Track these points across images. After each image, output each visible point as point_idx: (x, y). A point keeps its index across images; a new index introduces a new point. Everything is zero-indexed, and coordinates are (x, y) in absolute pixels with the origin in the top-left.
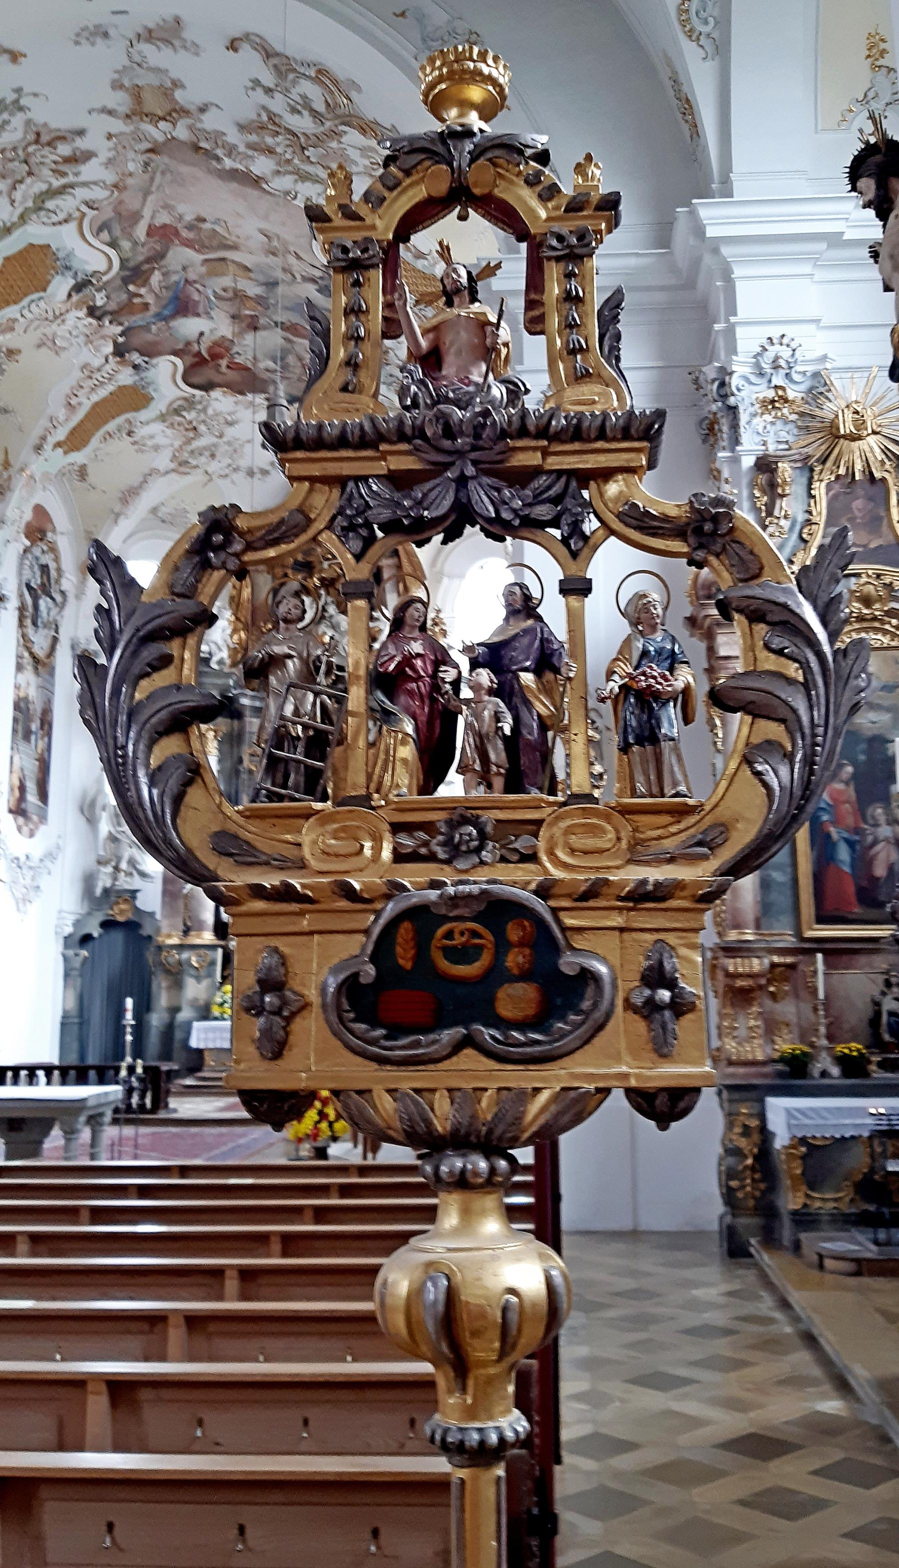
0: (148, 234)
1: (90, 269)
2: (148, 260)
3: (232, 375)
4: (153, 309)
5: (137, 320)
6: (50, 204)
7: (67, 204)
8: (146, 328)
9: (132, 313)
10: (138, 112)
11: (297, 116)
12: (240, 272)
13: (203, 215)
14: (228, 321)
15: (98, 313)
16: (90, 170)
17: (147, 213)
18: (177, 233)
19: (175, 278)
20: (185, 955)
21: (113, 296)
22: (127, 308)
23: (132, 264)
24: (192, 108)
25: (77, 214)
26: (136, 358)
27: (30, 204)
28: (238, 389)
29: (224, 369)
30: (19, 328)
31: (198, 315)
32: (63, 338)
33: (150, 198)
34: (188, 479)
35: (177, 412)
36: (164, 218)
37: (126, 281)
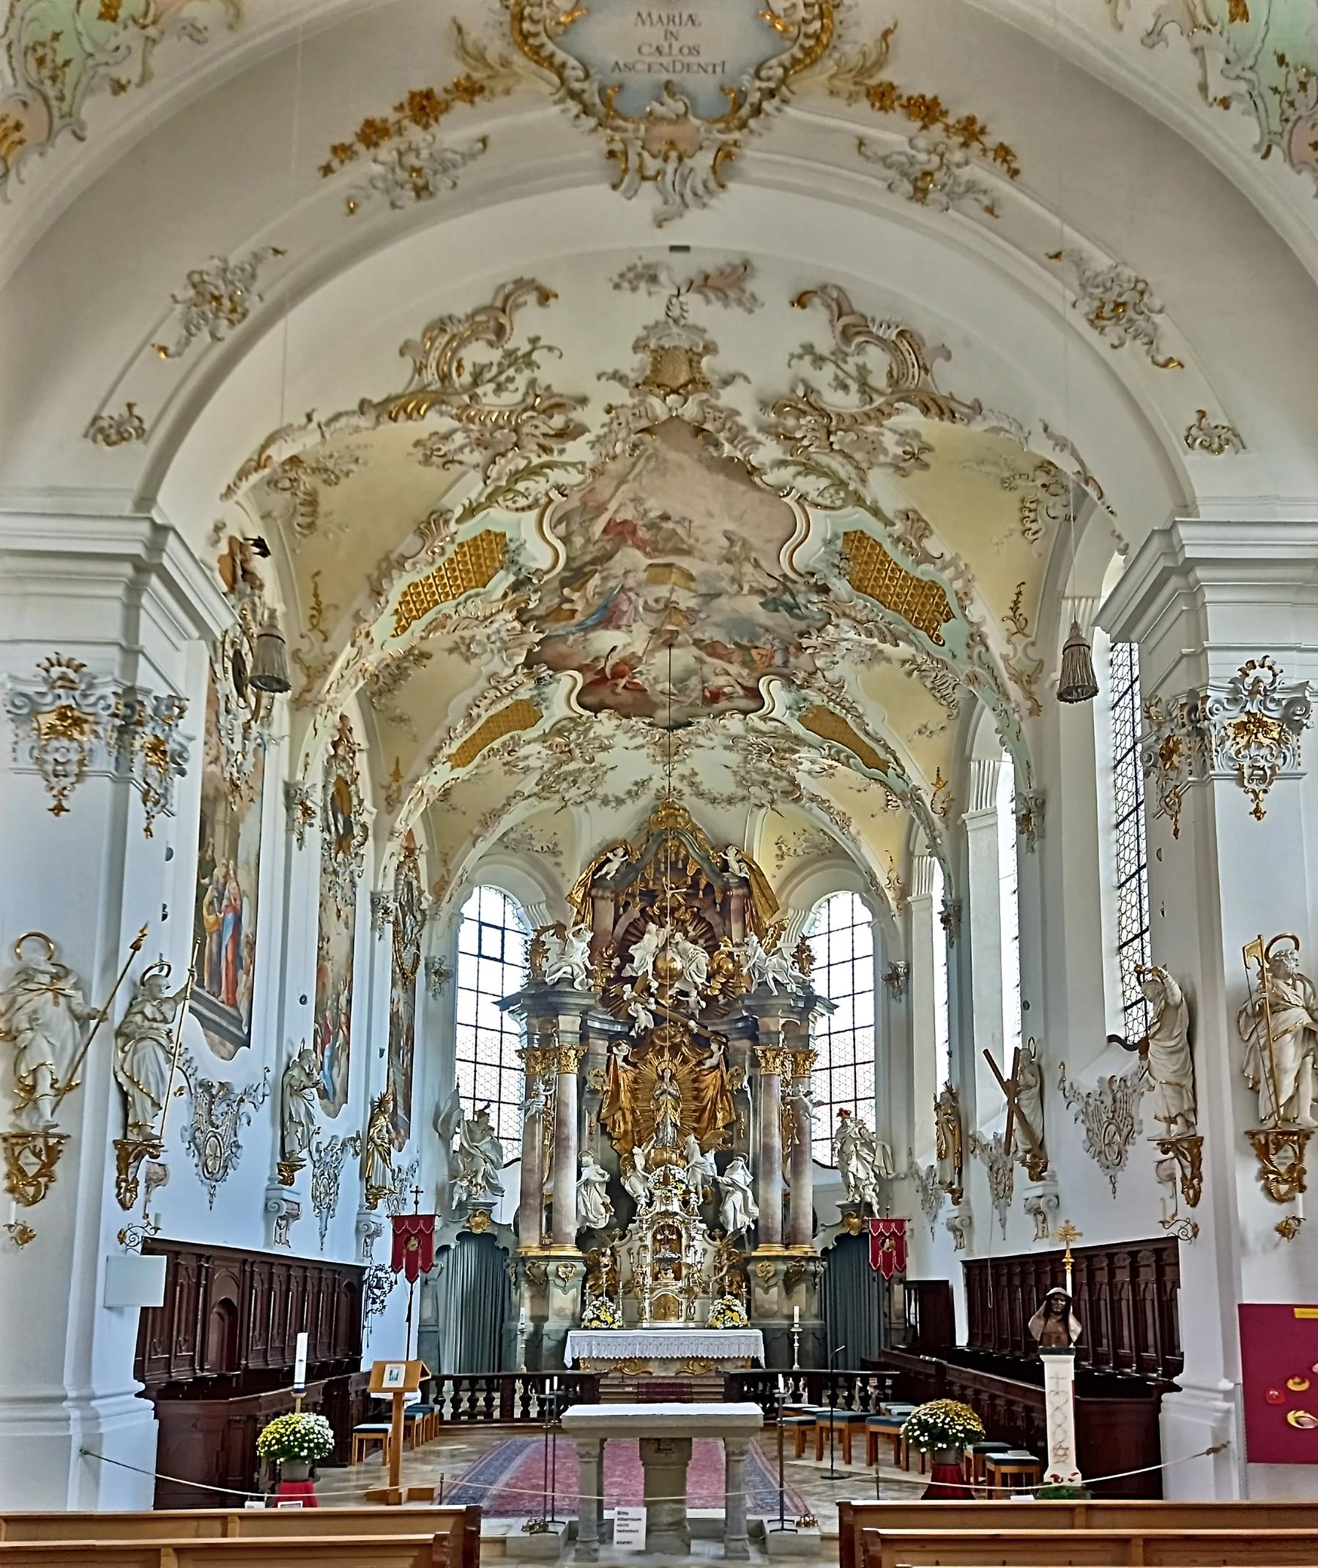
0: (605, 531)
1: (535, 565)
2: (594, 562)
3: (626, 697)
4: (579, 617)
5: (558, 628)
6: (521, 486)
7: (536, 486)
8: (563, 638)
9: (557, 620)
10: (653, 382)
11: (840, 393)
12: (682, 581)
13: (670, 512)
14: (646, 635)
15: (524, 618)
16: (577, 450)
17: (613, 506)
18: (634, 532)
19: (612, 584)
20: (552, 1267)
21: (545, 599)
22: (554, 614)
23: (576, 564)
24: (714, 380)
25: (543, 501)
26: (544, 671)
27: (503, 483)
28: (624, 712)
29: (619, 690)
30: (450, 625)
31: (618, 627)
32: (479, 643)
33: (624, 488)
34: (546, 804)
35: (560, 732)
36: (628, 514)
37: (564, 583)
